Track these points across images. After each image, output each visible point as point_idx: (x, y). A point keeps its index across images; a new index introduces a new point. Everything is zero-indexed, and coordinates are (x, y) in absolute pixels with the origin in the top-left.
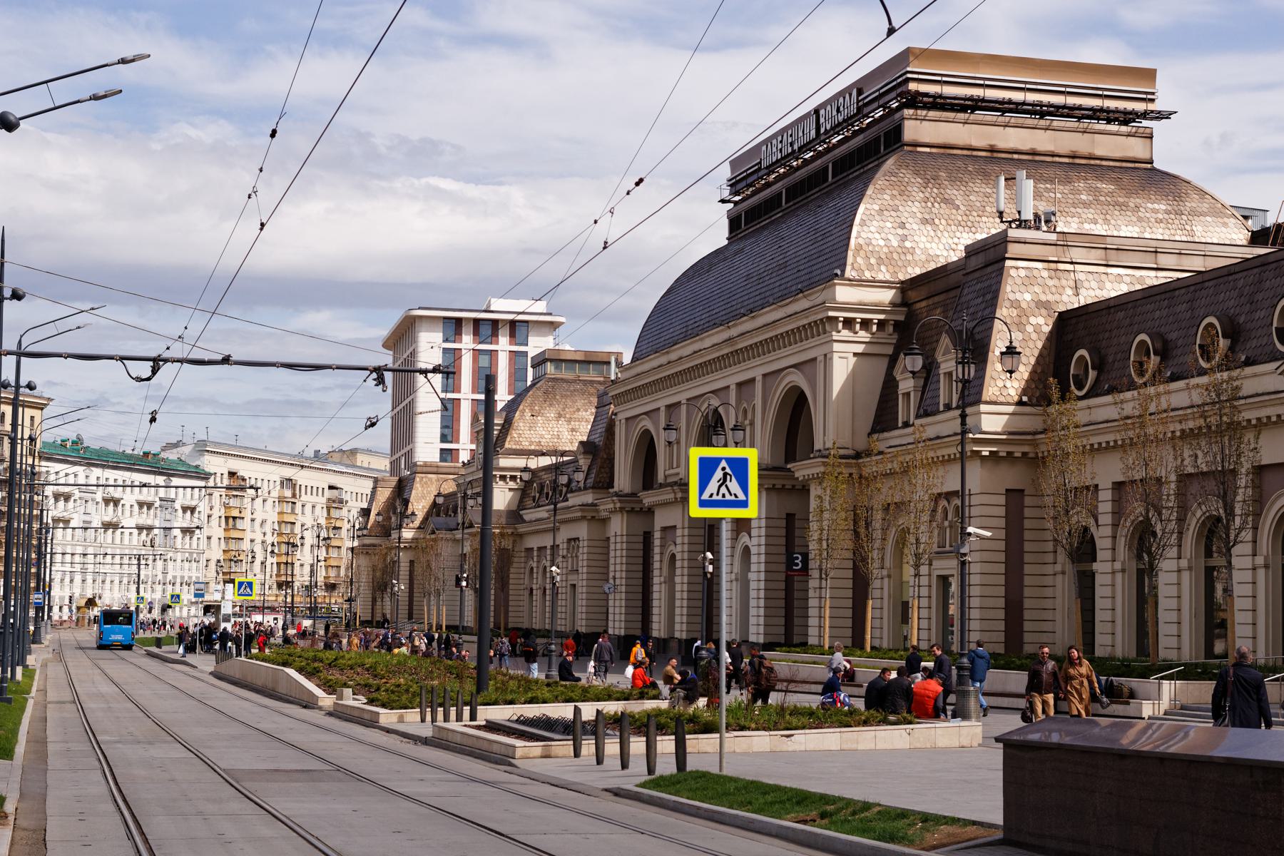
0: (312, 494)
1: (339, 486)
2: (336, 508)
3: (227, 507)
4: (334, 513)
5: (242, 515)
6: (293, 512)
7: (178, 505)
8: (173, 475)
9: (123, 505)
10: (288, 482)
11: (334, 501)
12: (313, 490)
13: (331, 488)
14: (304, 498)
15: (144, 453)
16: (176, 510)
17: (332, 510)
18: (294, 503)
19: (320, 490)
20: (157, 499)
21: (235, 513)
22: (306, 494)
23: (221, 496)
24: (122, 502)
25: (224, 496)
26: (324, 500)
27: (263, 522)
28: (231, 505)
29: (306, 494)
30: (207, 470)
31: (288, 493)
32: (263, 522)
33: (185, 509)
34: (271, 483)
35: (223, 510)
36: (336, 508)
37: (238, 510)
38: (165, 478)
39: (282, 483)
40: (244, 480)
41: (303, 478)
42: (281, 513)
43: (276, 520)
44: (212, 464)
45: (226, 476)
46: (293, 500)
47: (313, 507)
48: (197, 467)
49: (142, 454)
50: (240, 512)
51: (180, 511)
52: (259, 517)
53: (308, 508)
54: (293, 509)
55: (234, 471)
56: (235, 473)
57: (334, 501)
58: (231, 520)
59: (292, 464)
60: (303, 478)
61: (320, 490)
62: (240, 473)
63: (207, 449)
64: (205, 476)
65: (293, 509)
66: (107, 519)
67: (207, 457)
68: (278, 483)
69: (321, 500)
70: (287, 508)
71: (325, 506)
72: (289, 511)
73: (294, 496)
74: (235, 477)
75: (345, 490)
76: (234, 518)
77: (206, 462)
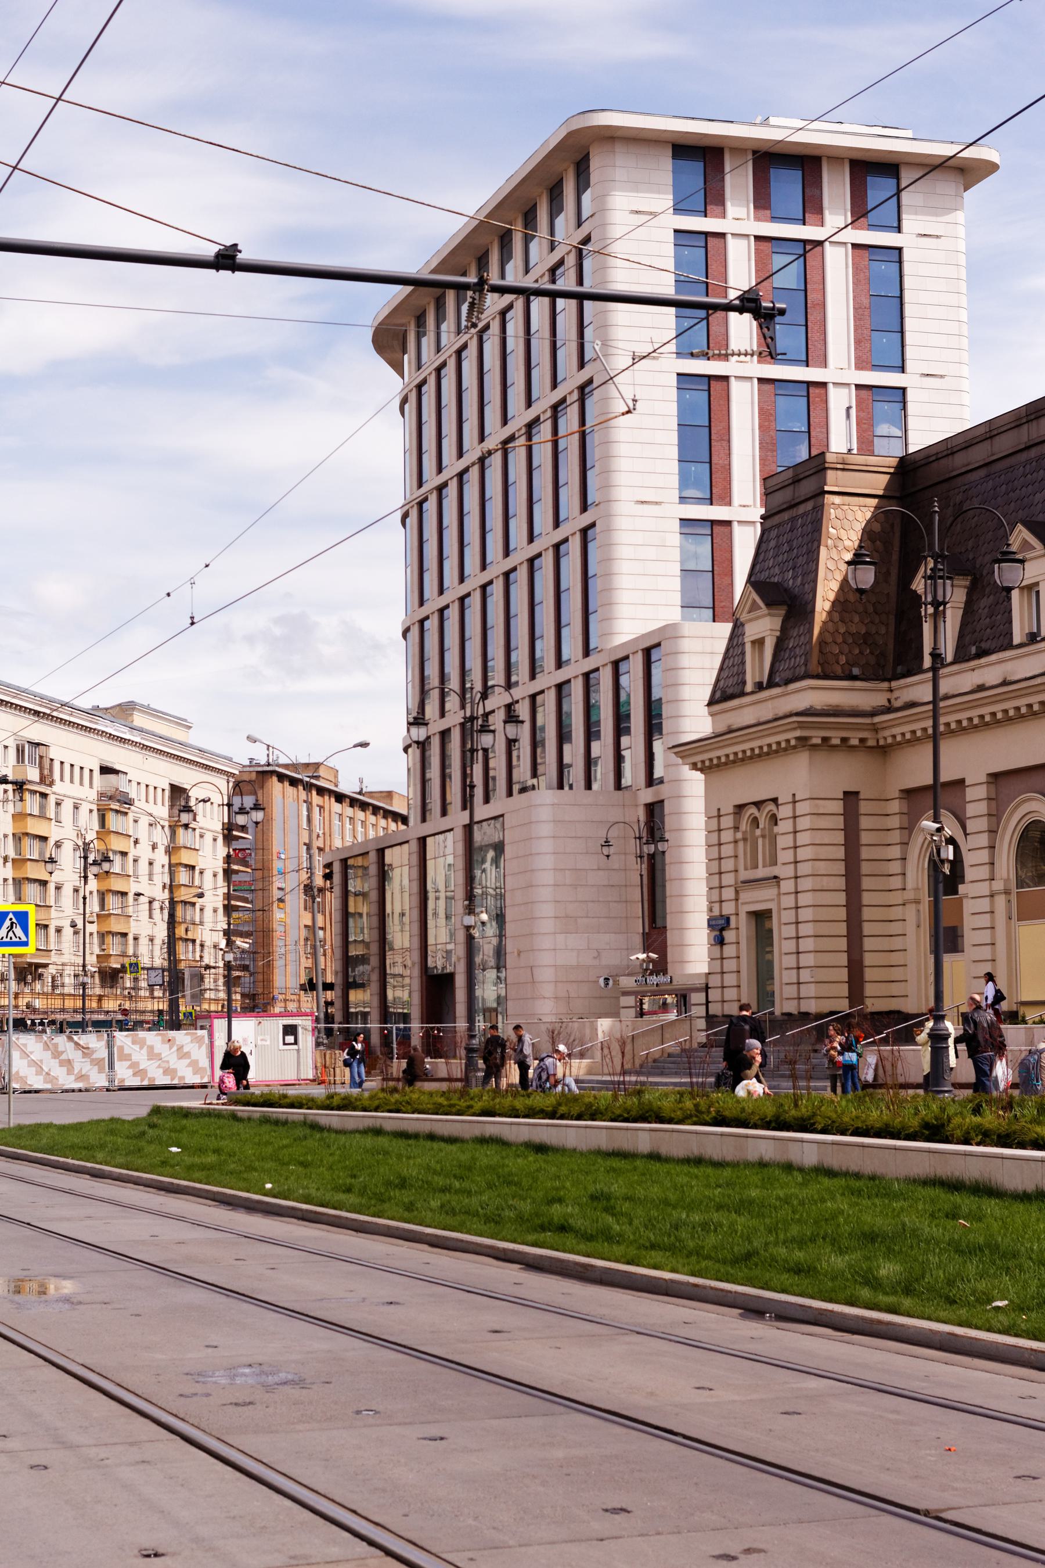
0: (72, 781)
1: (117, 767)
2: (117, 811)
4: (114, 822)
6: (42, 816)
11: (111, 798)
12: (76, 772)
13: (105, 770)
14: (59, 788)
17: (111, 817)
18: (44, 796)
19: (86, 773)
22: (62, 780)
26: (93, 795)
29: (62, 780)
31: (33, 774)
36: (117, 811)
39: (20, 751)
42: (19, 817)
43: (10, 832)
47: (76, 807)
53: (67, 807)
54: (43, 808)
57: (111, 798)
59: (37, 713)
61: (86, 773)
65: (43, 808)
68: (12, 753)
69: (89, 794)
70: (32, 804)
71: (95, 807)
72: (36, 812)
73: (42, 780)
75: (129, 777)
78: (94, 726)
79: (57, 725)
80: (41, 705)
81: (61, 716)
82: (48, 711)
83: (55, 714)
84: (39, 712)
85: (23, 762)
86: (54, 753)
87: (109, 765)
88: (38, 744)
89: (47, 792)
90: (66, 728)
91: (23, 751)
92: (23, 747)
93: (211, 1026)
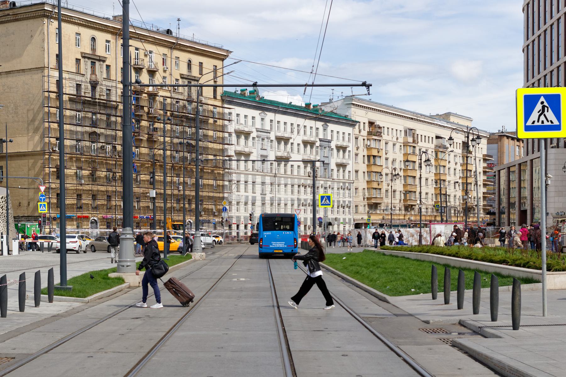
0: (425, 142)
1: (442, 136)
2: (441, 152)
3: (369, 148)
4: (440, 155)
5: (380, 155)
7: (333, 145)
8: (329, 121)
9: (292, 144)
10: (410, 132)
11: (440, 147)
12: (426, 138)
13: (437, 137)
14: (420, 144)
15: (306, 105)
16: (332, 149)
17: (439, 154)
18: (414, 147)
19: (431, 139)
20: (318, 140)
21: (375, 153)
23: (364, 140)
24: (291, 141)
25: (366, 140)
26: (433, 146)
27: (394, 161)
28: (372, 146)
30: (353, 119)
31: (410, 140)
32: (394, 161)
33: (339, 148)
34: (398, 131)
35: (365, 150)
36: (441, 152)
37: (377, 150)
38: (323, 123)
39: (406, 132)
40: (380, 128)
41: (421, 129)
42: (406, 155)
43: (402, 160)
44: (357, 114)
45: (367, 125)
46: (414, 145)
48: (346, 116)
49: (304, 105)
50: (378, 152)
51: (335, 151)
52: (391, 156)
55: (373, 121)
56: (374, 123)
57: (440, 147)
58: (372, 158)
59: (412, 119)
60: (421, 129)
61: (431, 139)
62: (377, 123)
63: (353, 102)
64: (352, 123)
66: (279, 154)
67: (353, 110)
68: (403, 133)
70: (410, 150)
71: (434, 150)
73: (414, 141)
74: (374, 126)
76: (374, 156)
77: (353, 113)
78: (433, 122)
79: (420, 122)
80: (413, 116)
81: (421, 119)
82: (416, 118)
83: (418, 118)
84: (413, 118)
85: (407, 136)
86: (418, 132)
87: (439, 135)
88: (412, 129)
89: (415, 146)
90: (423, 123)
91: (407, 132)
92: (407, 130)
93: (430, 227)
